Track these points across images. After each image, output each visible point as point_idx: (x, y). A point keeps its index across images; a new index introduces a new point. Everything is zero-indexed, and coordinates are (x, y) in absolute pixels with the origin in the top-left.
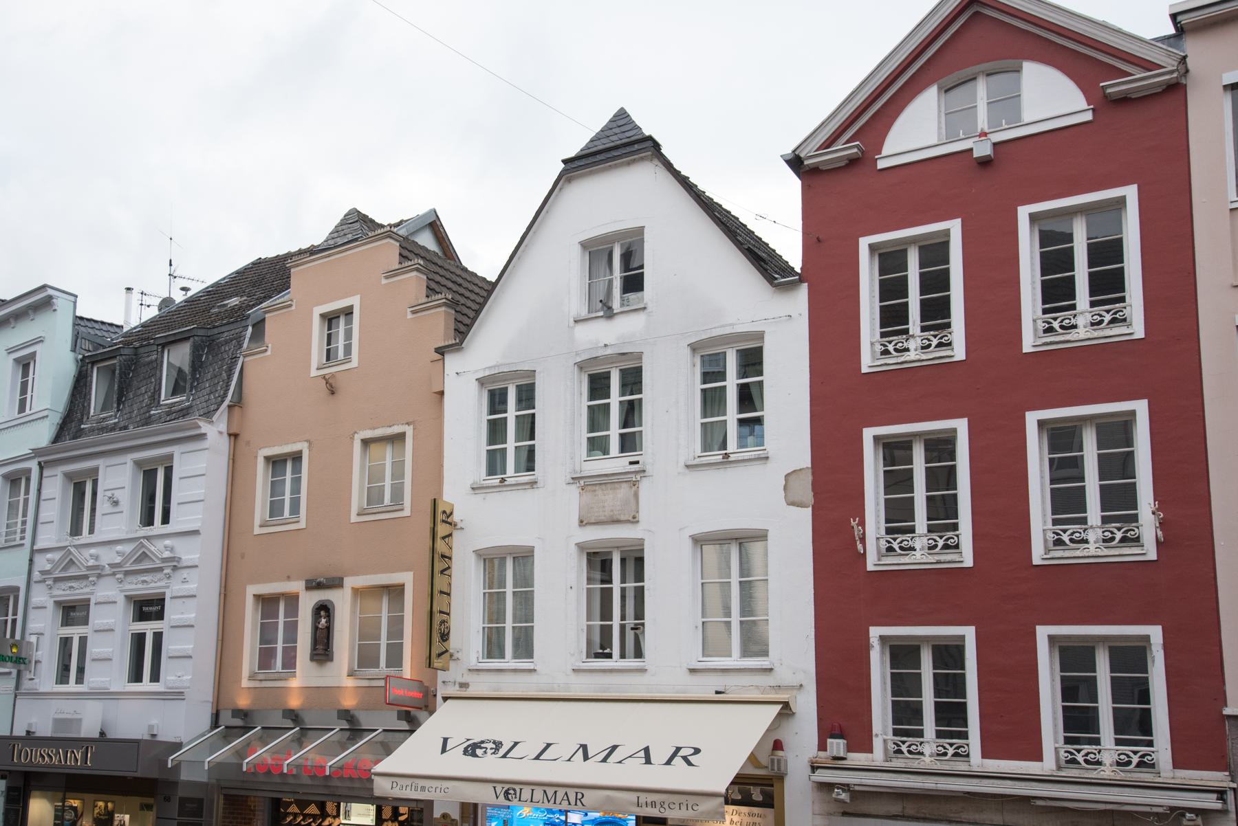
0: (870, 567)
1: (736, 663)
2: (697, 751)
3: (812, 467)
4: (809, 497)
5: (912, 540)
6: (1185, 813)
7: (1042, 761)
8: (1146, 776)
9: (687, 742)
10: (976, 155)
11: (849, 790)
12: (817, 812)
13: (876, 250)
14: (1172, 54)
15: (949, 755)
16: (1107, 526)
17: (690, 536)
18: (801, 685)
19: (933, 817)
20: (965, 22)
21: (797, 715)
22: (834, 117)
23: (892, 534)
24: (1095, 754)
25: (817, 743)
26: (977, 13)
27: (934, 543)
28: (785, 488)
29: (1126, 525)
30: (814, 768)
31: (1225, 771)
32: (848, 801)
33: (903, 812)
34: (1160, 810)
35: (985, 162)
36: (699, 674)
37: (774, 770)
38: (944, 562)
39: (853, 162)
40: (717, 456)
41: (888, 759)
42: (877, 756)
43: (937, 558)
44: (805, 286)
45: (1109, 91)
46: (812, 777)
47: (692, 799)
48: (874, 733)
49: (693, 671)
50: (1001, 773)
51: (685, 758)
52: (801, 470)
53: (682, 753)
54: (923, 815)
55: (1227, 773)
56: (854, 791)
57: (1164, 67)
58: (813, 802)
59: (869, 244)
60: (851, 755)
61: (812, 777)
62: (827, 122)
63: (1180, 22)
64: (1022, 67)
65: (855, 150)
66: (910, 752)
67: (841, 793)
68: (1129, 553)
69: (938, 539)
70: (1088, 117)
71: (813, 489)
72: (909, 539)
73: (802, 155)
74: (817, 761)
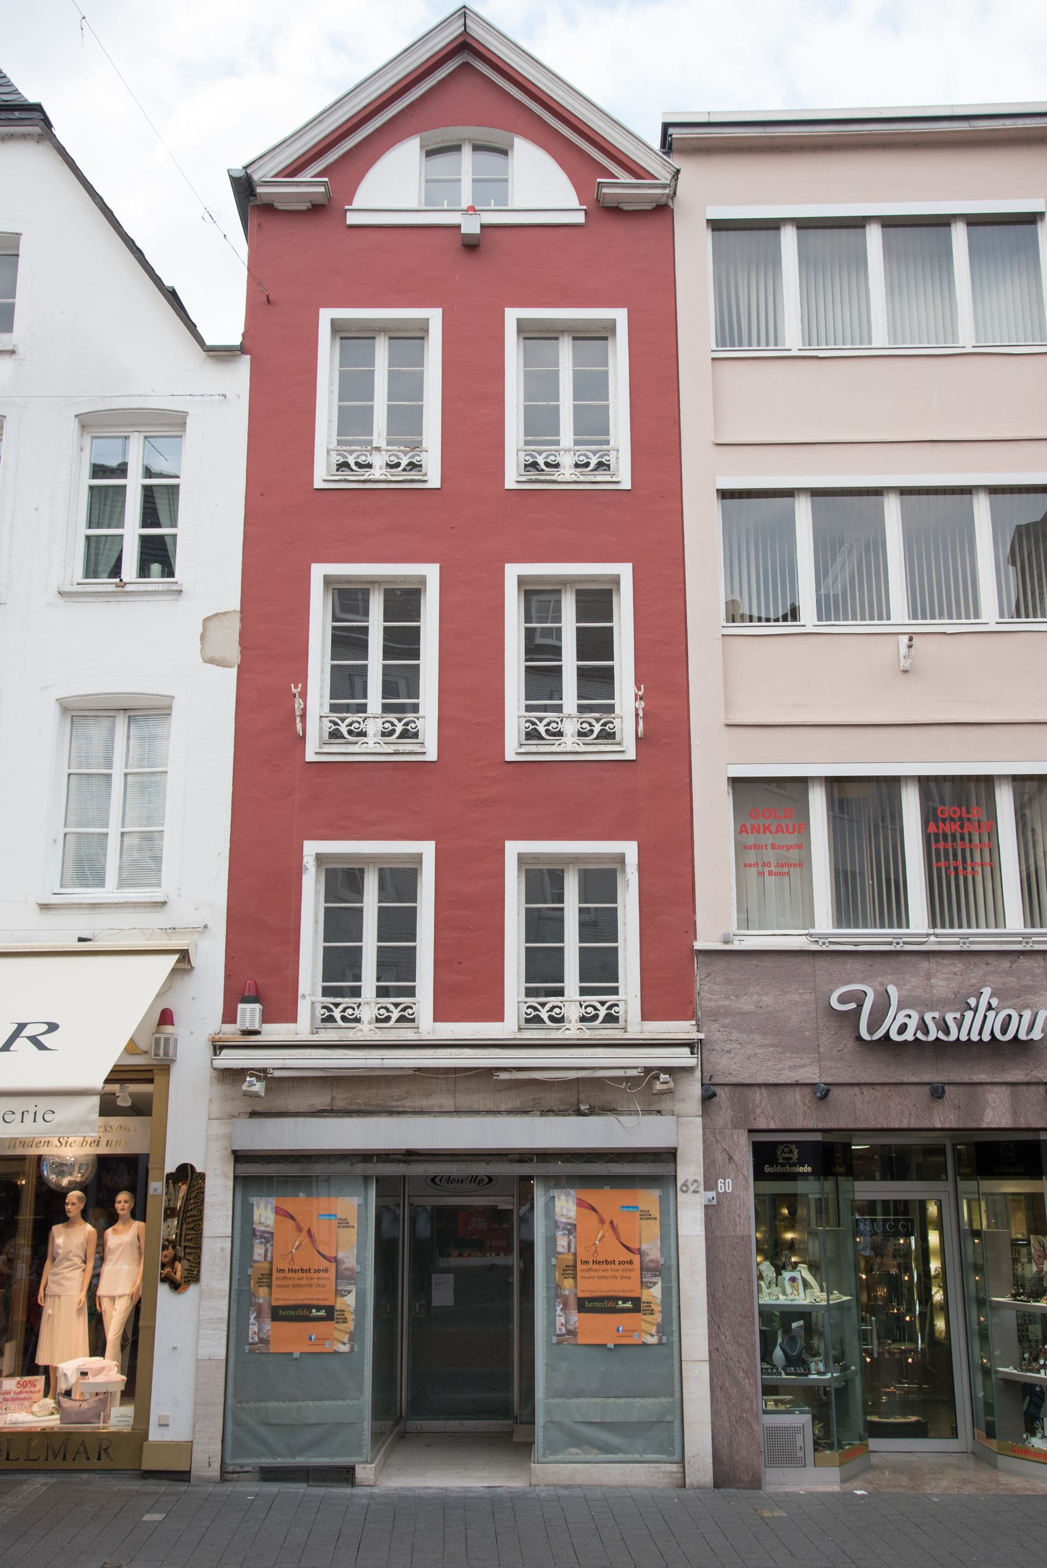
0: (310, 757)
1: (111, 895)
2: (53, 1027)
3: (242, 612)
4: (233, 651)
5: (364, 721)
6: (660, 1074)
7: (503, 1020)
8: (611, 1033)
9: (36, 1016)
10: (463, 231)
11: (266, 1078)
12: (213, 1116)
13: (338, 331)
14: (667, 164)
15: (394, 1019)
16: (586, 715)
17: (57, 700)
18: (206, 927)
19: (370, 1108)
20: (454, 70)
21: (196, 972)
22: (299, 137)
23: (340, 713)
24: (560, 1008)
25: (221, 1012)
26: (466, 65)
27: (391, 728)
28: (203, 637)
29: (606, 715)
30: (218, 1047)
31: (692, 1019)
32: (263, 1094)
33: (331, 1104)
34: (634, 1073)
35: (471, 246)
36: (53, 912)
37: (158, 1055)
38: (403, 753)
39: (317, 209)
40: (104, 583)
41: (315, 1030)
42: (302, 1028)
43: (390, 749)
44: (247, 359)
45: (605, 190)
46: (215, 1062)
47: (44, 1104)
48: (300, 993)
49: (45, 907)
50: (456, 1040)
51: (34, 1040)
52: (225, 613)
53: (28, 1032)
54: (356, 1107)
55: (694, 1022)
56: (273, 1078)
57: (657, 179)
58: (210, 1101)
59: (332, 320)
60: (267, 1028)
61: (215, 1062)
62: (290, 141)
63: (670, 135)
64: (512, 146)
65: (322, 189)
66: (344, 1018)
67: (255, 1082)
68: (605, 752)
69: (396, 722)
70: (580, 218)
71: (241, 644)
72: (361, 720)
73: (256, 177)
74: (220, 1038)
